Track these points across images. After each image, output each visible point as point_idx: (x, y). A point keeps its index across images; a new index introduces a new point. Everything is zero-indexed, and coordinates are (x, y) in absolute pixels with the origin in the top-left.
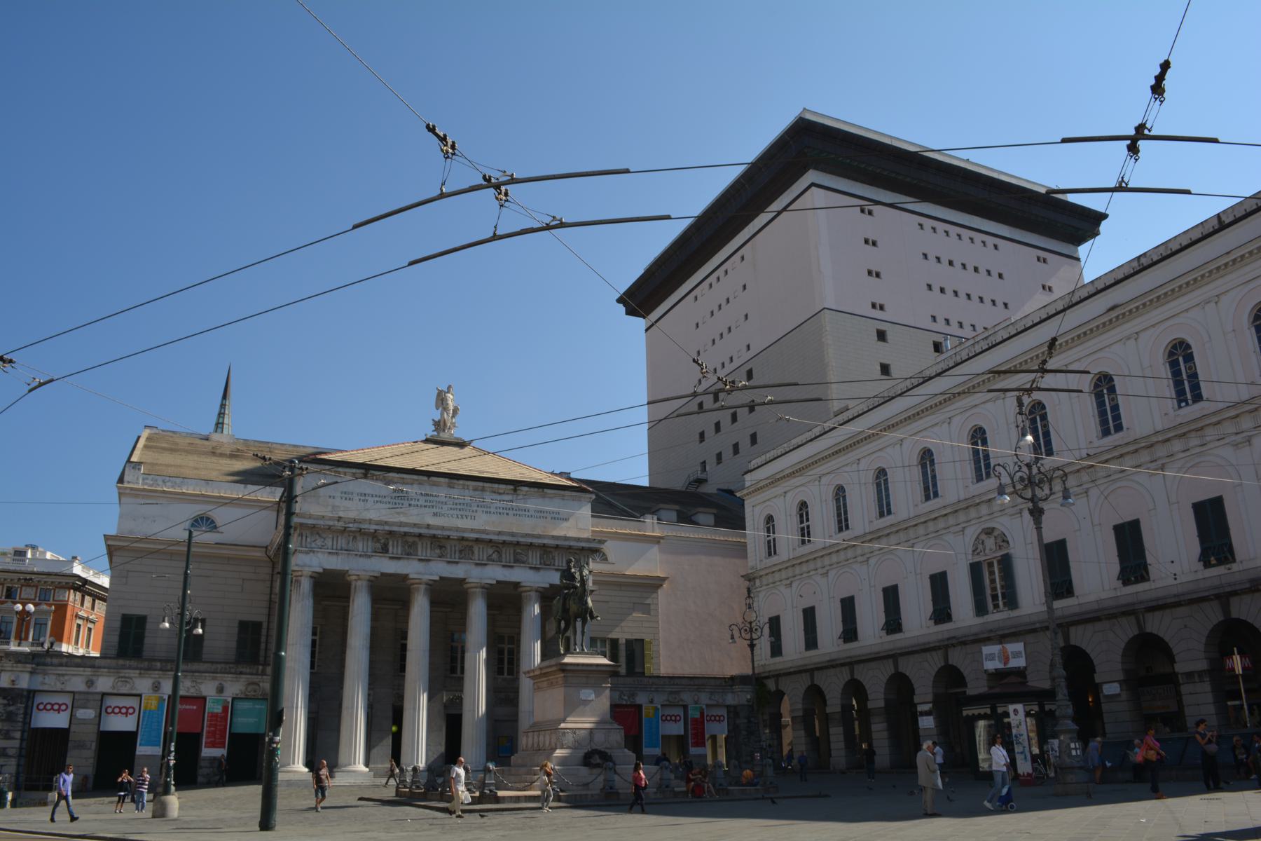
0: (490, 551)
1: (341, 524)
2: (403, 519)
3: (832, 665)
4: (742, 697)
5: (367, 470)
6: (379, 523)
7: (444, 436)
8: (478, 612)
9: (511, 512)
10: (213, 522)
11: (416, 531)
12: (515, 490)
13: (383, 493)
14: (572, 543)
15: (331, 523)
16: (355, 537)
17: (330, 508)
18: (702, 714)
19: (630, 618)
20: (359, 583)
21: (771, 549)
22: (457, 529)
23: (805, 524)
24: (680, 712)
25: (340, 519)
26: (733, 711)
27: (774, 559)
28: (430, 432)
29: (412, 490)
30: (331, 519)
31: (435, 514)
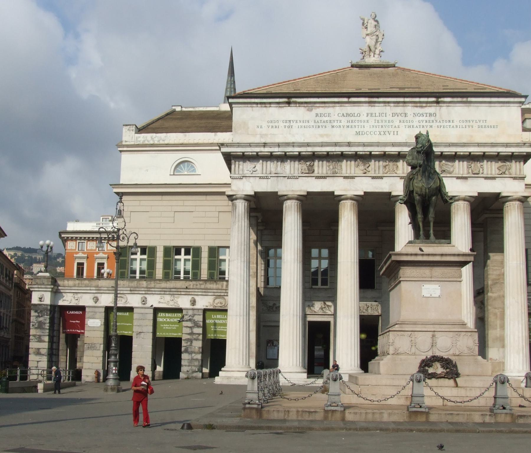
2: (325, 140)
6: (301, 145)
7: (371, 60)
9: (434, 124)
10: (192, 167)
12: (438, 102)
13: (306, 118)
15: (257, 149)
17: (258, 136)
22: (378, 144)
25: (265, 145)
28: (357, 59)
29: (335, 112)
30: (257, 145)
31: (358, 133)
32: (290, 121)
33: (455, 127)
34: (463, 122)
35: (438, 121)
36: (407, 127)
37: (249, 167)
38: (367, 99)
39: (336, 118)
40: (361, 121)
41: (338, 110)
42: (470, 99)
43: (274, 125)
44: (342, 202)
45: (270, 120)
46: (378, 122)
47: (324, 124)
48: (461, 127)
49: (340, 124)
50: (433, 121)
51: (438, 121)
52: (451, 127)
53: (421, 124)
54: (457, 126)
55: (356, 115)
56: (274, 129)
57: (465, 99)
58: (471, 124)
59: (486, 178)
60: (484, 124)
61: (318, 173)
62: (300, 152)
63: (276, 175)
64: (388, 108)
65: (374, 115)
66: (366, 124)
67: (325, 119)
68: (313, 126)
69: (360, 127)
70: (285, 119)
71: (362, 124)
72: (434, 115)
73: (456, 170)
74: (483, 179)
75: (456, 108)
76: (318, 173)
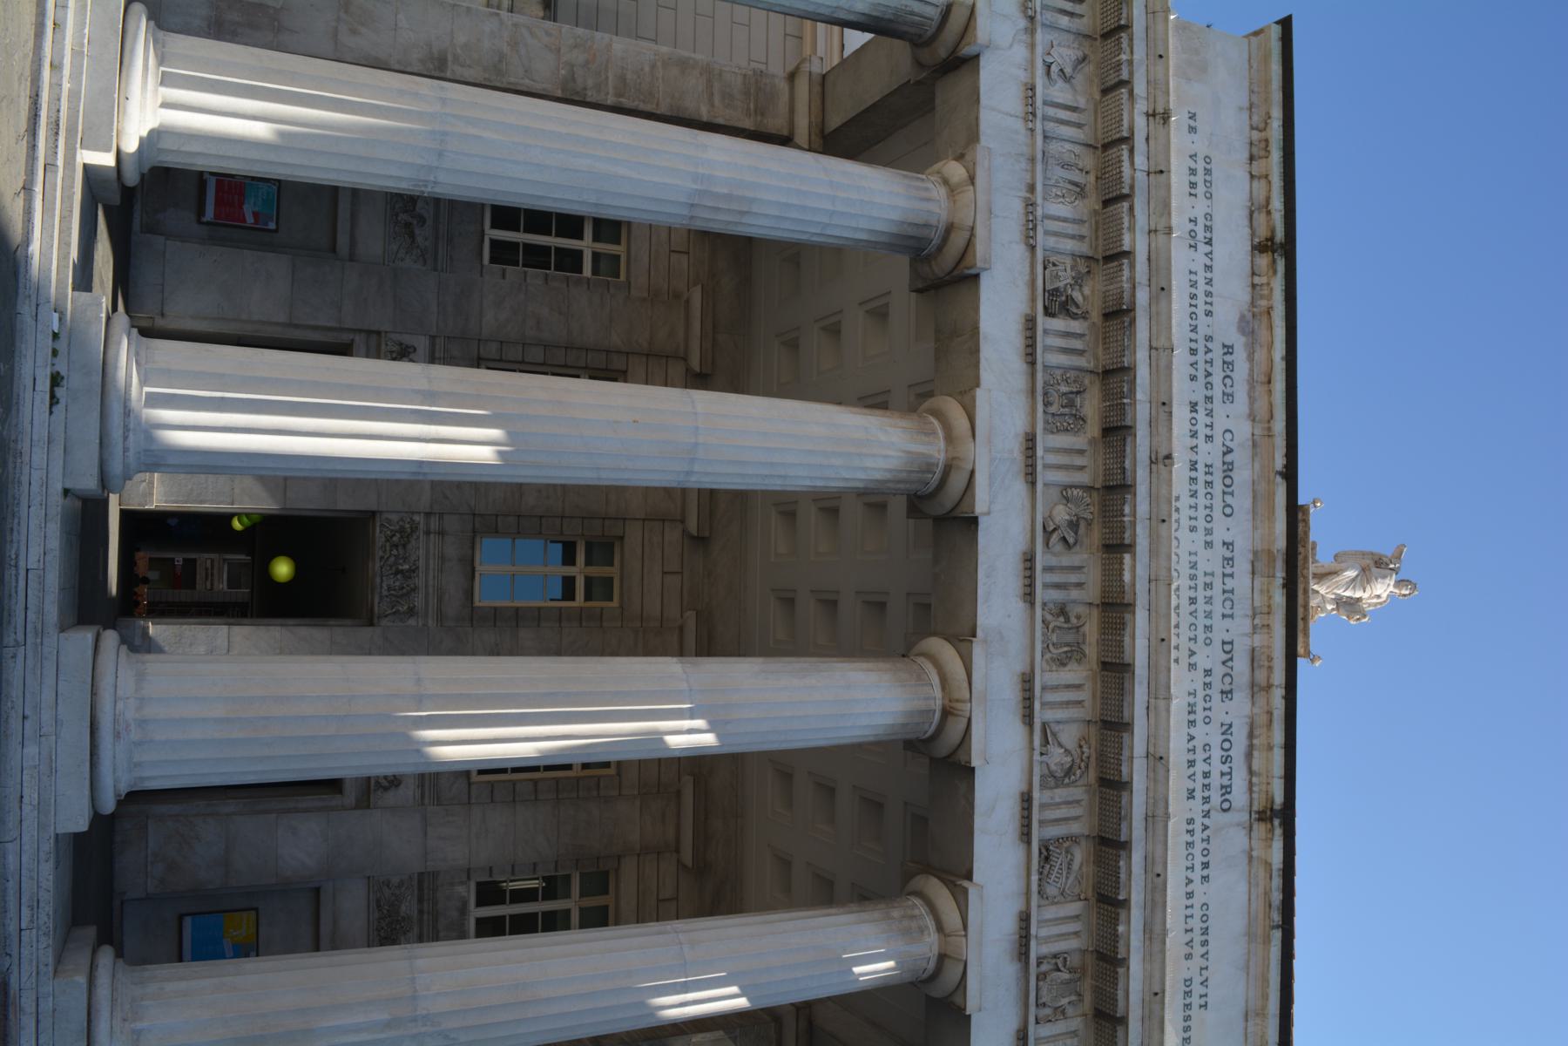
0: (1069, 736)
1: (1140, 122)
5: (1279, 248)
8: (843, 701)
9: (1197, 806)
11: (1142, 412)
15: (1140, 88)
16: (1080, 191)
20: (940, 192)
22: (1160, 581)
30: (1158, 86)
32: (1209, 242)
33: (1189, 889)
34: (1205, 918)
35: (1206, 821)
36: (1191, 699)
37: (1066, 52)
38: (1281, 543)
39: (1220, 423)
40: (1209, 518)
41: (1243, 430)
42: (1277, 935)
43: (1200, 178)
44: (936, 422)
45: (1213, 166)
46: (1208, 586)
47: (1201, 374)
48: (1189, 911)
49: (1201, 437)
50: (1206, 800)
51: (1206, 821)
53: (1200, 756)
54: (1190, 895)
55: (1229, 499)
56: (1186, 179)
57: (1277, 917)
58: (1198, 950)
60: (1195, 1001)
61: (1045, 332)
62: (1128, 254)
63: (1039, 156)
64: (1247, 627)
65: (1228, 570)
66: (1200, 536)
67: (1217, 379)
68: (1194, 329)
69: (1192, 513)
70: (1217, 224)
71: (1201, 524)
72: (1226, 805)
73: (1051, 912)
74: (1011, 1023)
75: (1242, 887)
76: (1045, 332)
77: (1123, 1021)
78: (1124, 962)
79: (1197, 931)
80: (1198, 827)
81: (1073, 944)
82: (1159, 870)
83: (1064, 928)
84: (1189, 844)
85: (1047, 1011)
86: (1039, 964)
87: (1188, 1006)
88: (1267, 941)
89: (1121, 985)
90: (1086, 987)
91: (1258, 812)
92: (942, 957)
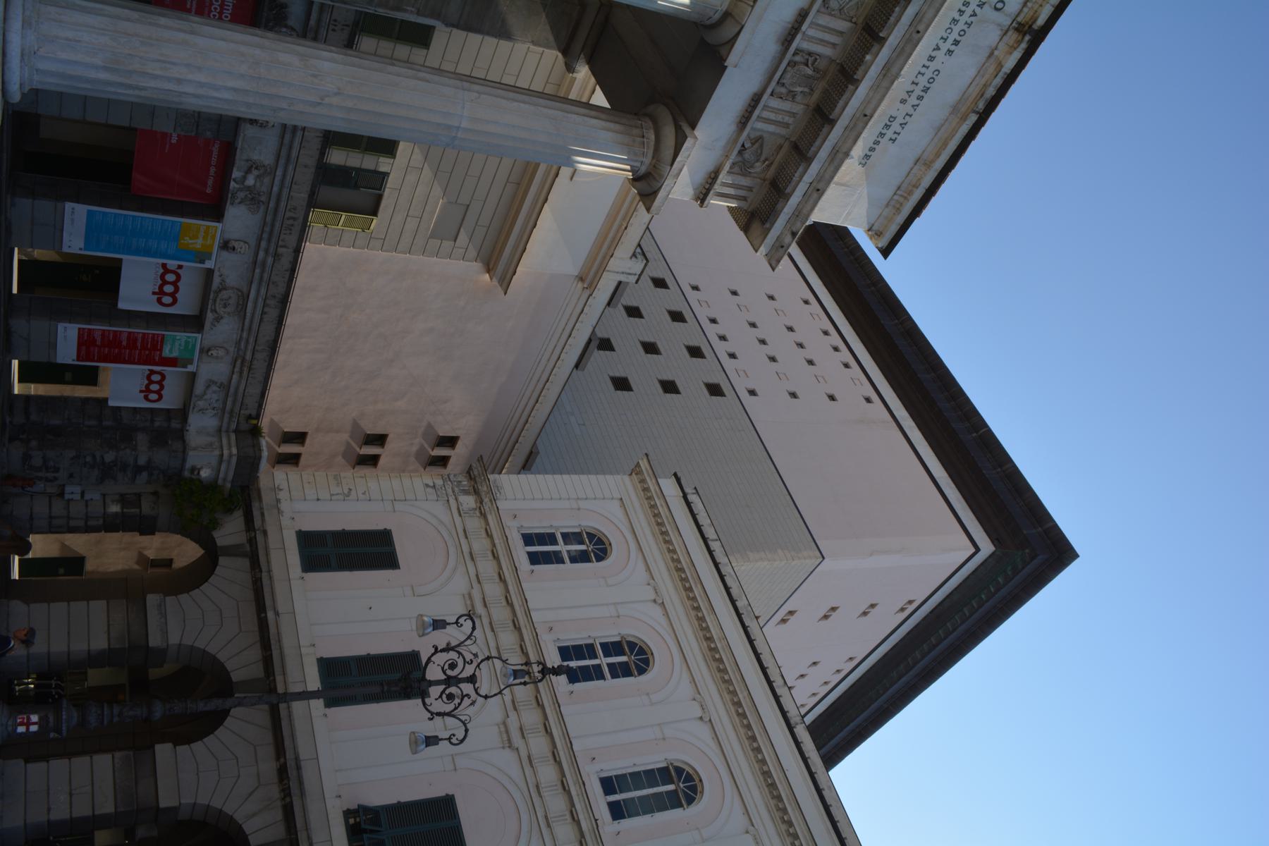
3: (288, 776)
4: (206, 454)
14: (815, 168)
18: (172, 362)
19: (437, 190)
21: (542, 549)
23: (604, 661)
24: (186, 304)
26: (168, 428)
27: (521, 553)
34: (931, 80)
35: (978, 10)
48: (923, 70)
51: (978, 10)
52: (941, 43)
54: (931, 58)
57: (981, 106)
58: (913, 100)
59: (756, 100)
60: (889, 134)
73: (824, 20)
74: (753, 86)
75: (972, 72)
77: (832, 123)
78: (856, 83)
79: (921, 87)
80: (969, 11)
81: (827, 51)
82: (921, 28)
83: (828, 37)
84: (955, 21)
85: (783, 90)
86: (795, 54)
87: (882, 135)
88: (964, 118)
89: (844, 97)
90: (820, 87)
91: (1019, 24)
92: (727, 15)
